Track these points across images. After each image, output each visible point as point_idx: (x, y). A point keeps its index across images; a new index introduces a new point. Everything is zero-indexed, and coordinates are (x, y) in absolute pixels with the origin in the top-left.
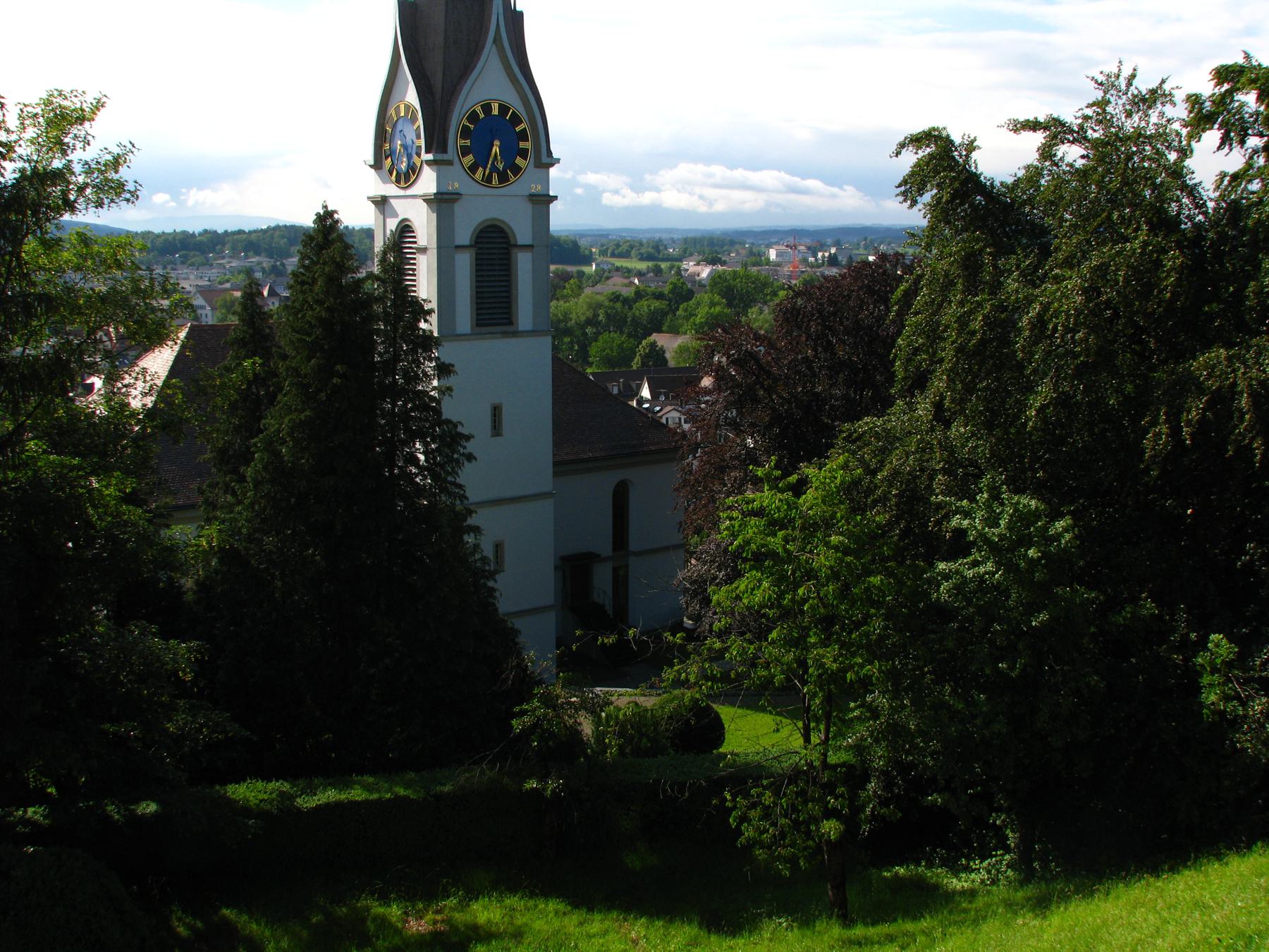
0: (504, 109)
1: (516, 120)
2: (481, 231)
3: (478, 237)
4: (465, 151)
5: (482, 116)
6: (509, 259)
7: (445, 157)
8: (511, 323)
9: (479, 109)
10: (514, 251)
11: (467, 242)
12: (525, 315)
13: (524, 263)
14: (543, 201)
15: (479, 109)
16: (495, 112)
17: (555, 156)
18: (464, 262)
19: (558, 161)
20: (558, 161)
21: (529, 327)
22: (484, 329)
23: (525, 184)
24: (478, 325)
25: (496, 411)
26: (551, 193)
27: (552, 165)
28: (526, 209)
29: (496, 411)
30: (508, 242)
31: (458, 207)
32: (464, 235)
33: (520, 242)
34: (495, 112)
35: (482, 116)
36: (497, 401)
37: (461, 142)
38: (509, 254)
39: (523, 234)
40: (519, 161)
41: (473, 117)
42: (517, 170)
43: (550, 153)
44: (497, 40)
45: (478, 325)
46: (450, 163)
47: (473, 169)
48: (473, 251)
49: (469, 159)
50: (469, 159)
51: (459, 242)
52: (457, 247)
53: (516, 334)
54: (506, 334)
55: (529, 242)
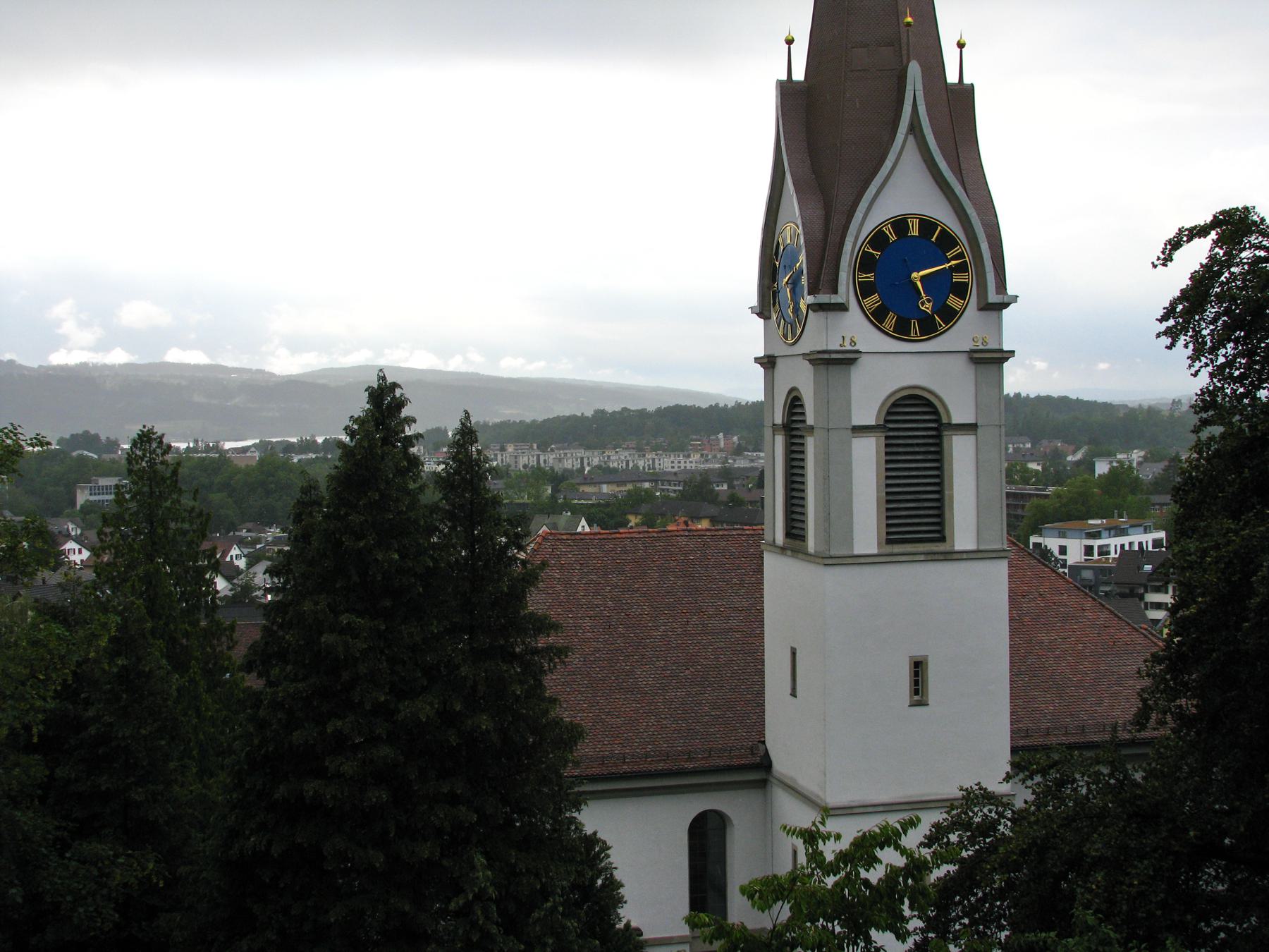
0: (928, 225)
1: (948, 240)
2: (894, 405)
3: (889, 413)
5: (893, 238)
6: (940, 445)
7: (835, 299)
8: (942, 539)
9: (888, 230)
11: (871, 421)
14: (991, 360)
15: (888, 230)
17: (1011, 289)
21: (971, 546)
22: (897, 549)
23: (966, 332)
24: (889, 542)
25: (918, 667)
26: (1006, 348)
27: (1006, 305)
29: (918, 667)
30: (938, 421)
33: (954, 421)
35: (893, 238)
36: (918, 652)
37: (863, 277)
38: (939, 437)
40: (953, 301)
41: (878, 239)
44: (915, 128)
49: (873, 301)
50: (873, 301)
51: (857, 422)
53: (951, 556)
55: (971, 420)
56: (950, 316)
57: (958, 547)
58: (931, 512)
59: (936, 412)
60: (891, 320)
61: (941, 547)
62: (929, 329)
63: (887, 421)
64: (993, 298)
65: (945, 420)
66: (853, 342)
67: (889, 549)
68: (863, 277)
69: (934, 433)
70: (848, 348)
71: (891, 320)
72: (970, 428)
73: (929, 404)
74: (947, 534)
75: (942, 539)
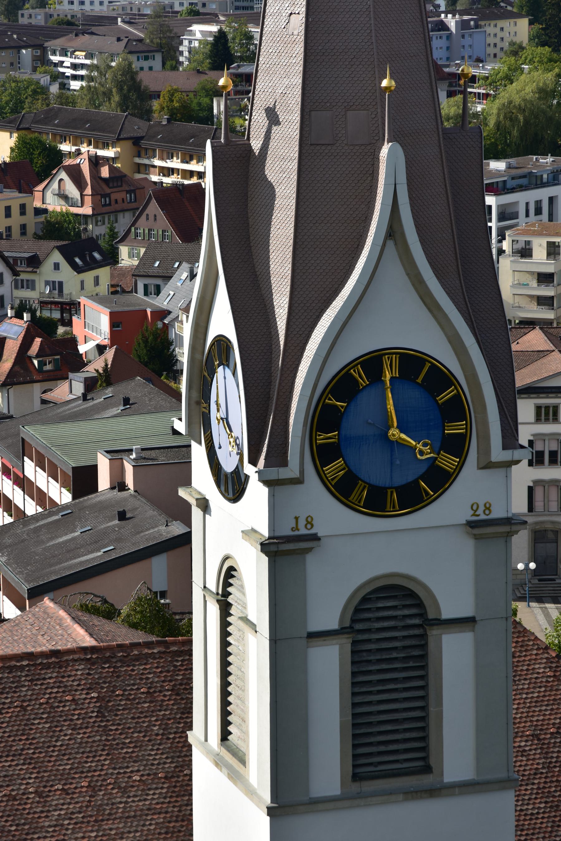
2: (365, 600)
3: (357, 610)
6: (424, 646)
8: (427, 769)
11: (334, 625)
12: (457, 750)
18: (327, 666)
24: (356, 777)
28: (466, 547)
30: (423, 615)
31: (312, 562)
32: (327, 609)
33: (446, 614)
38: (424, 636)
44: (393, 231)
45: (356, 777)
48: (346, 642)
51: (315, 626)
52: (312, 636)
54: (413, 794)
57: (449, 777)
58: (414, 735)
59: (420, 605)
61: (426, 780)
62: (412, 498)
63: (353, 621)
65: (431, 615)
66: (309, 522)
67: (355, 787)
68: (322, 438)
69: (417, 632)
70: (303, 531)
73: (412, 594)
74: (432, 761)
75: (427, 769)
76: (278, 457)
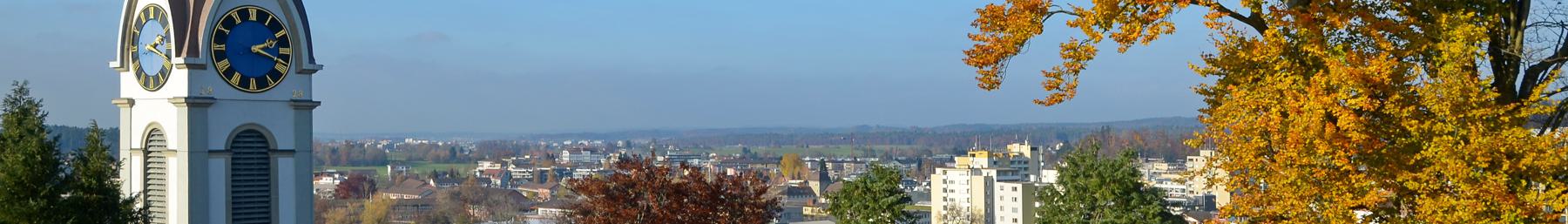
0: (262, 15)
1: (276, 26)
4: (220, 56)
5: (238, 21)
7: (198, 61)
9: (235, 15)
10: (272, 156)
13: (285, 169)
14: (306, 106)
15: (235, 15)
16: (253, 18)
18: (219, 169)
19: (321, 67)
20: (321, 67)
23: (288, 88)
28: (291, 113)
32: (219, 142)
34: (253, 18)
35: (238, 21)
39: (283, 137)
42: (277, 76)
43: (312, 60)
46: (203, 67)
47: (229, 74)
48: (229, 157)
49: (224, 64)
50: (224, 64)
56: (277, 76)
59: (266, 142)
60: (236, 78)
64: (306, 65)
71: (236, 78)
72: (291, 152)
73: (261, 136)
76: (193, 51)
